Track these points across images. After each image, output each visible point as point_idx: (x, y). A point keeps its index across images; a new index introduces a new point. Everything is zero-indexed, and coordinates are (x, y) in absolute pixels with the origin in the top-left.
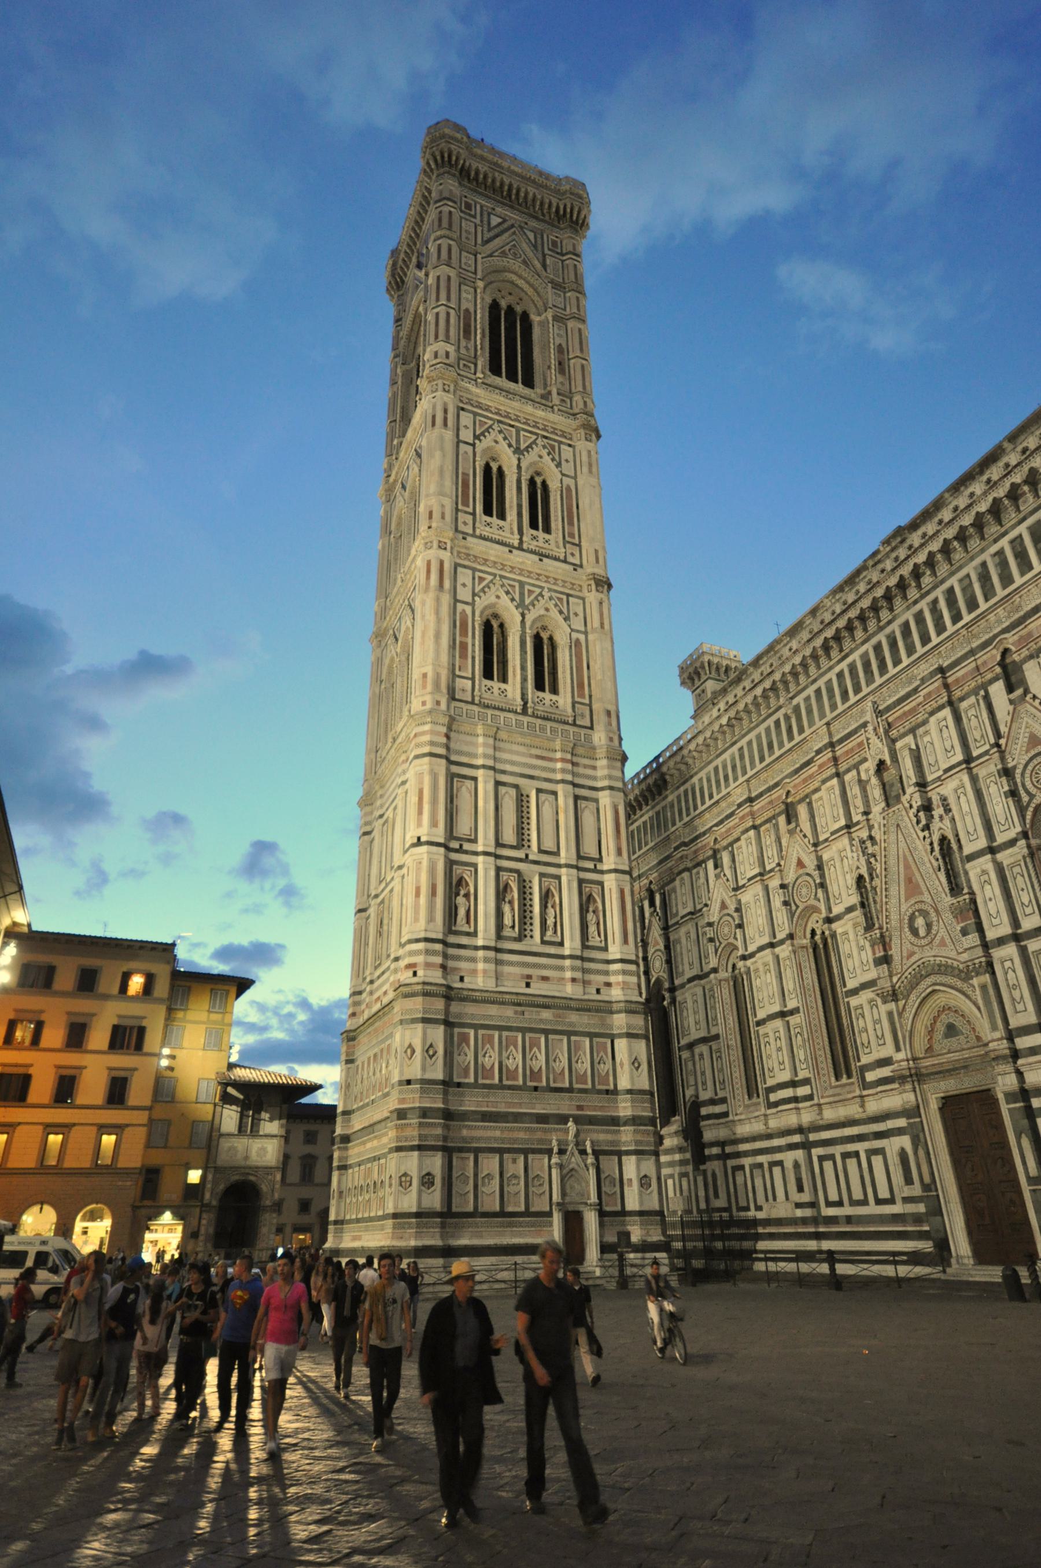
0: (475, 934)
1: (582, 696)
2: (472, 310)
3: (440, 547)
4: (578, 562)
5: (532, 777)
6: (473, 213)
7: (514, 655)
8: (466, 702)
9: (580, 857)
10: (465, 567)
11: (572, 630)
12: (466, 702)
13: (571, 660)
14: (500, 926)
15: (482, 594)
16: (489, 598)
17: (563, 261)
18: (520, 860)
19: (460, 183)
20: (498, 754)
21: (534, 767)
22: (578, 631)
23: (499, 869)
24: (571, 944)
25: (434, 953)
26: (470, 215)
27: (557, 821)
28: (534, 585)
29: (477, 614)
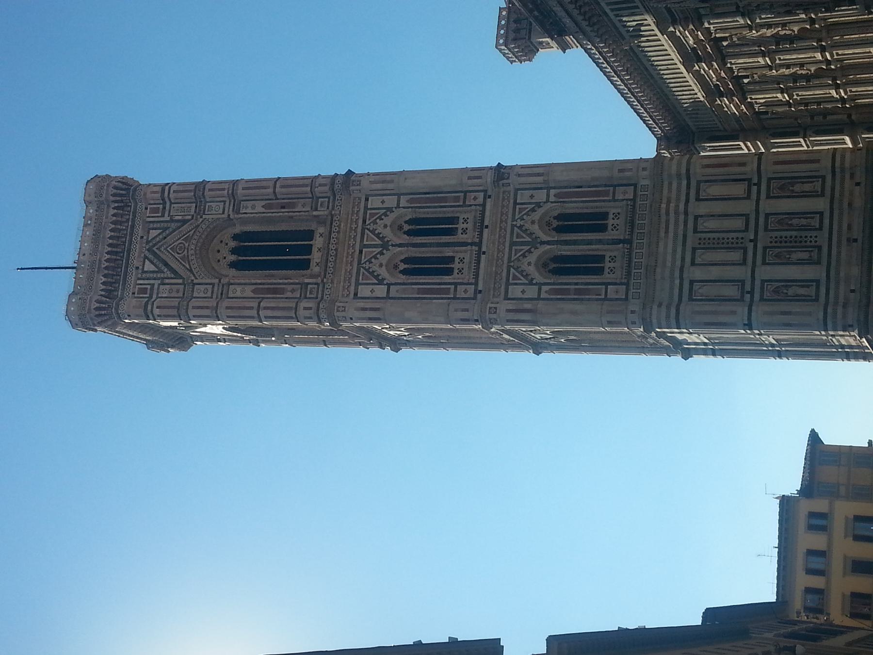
0: (818, 282)
3: (495, 313)
5: (685, 236)
7: (579, 250)
8: (627, 290)
9: (748, 197)
11: (547, 201)
12: (627, 290)
14: (810, 262)
15: (530, 278)
16: (531, 270)
17: (171, 203)
18: (755, 247)
19: (121, 299)
20: (669, 264)
22: (548, 195)
23: (764, 263)
24: (821, 204)
26: (152, 289)
27: (720, 216)
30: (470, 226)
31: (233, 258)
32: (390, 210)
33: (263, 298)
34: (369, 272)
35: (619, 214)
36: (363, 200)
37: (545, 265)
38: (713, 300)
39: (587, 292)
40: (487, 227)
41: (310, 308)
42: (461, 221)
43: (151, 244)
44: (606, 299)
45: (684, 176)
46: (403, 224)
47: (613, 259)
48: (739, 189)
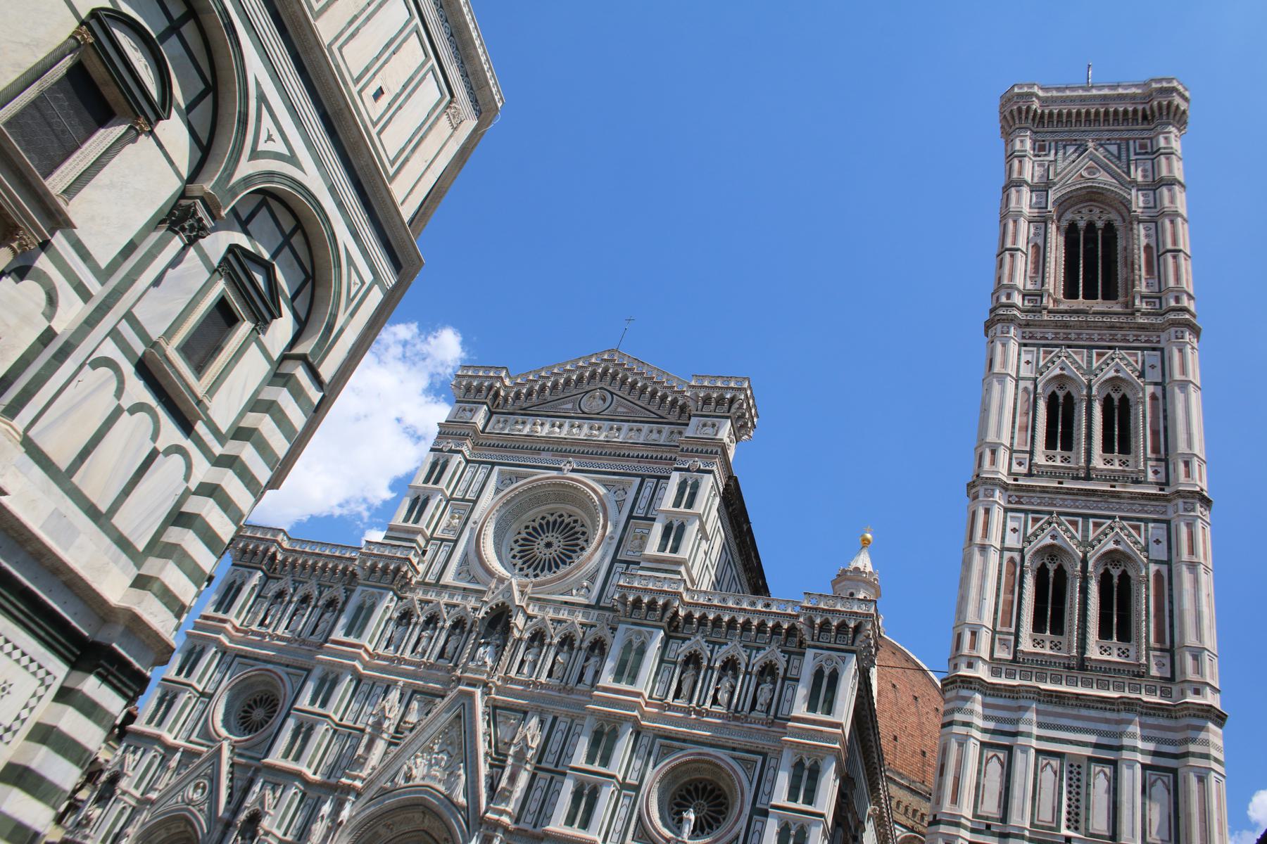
6: (1047, 152)
17: (1152, 159)
19: (1034, 132)
26: (1045, 155)
29: (1027, 558)
30: (1117, 466)
31: (1082, 224)
33: (1026, 255)
34: (1053, 357)
35: (1128, 656)
37: (1052, 559)
44: (994, 631)
45: (1181, 750)
46: (1121, 393)
47: (1055, 646)
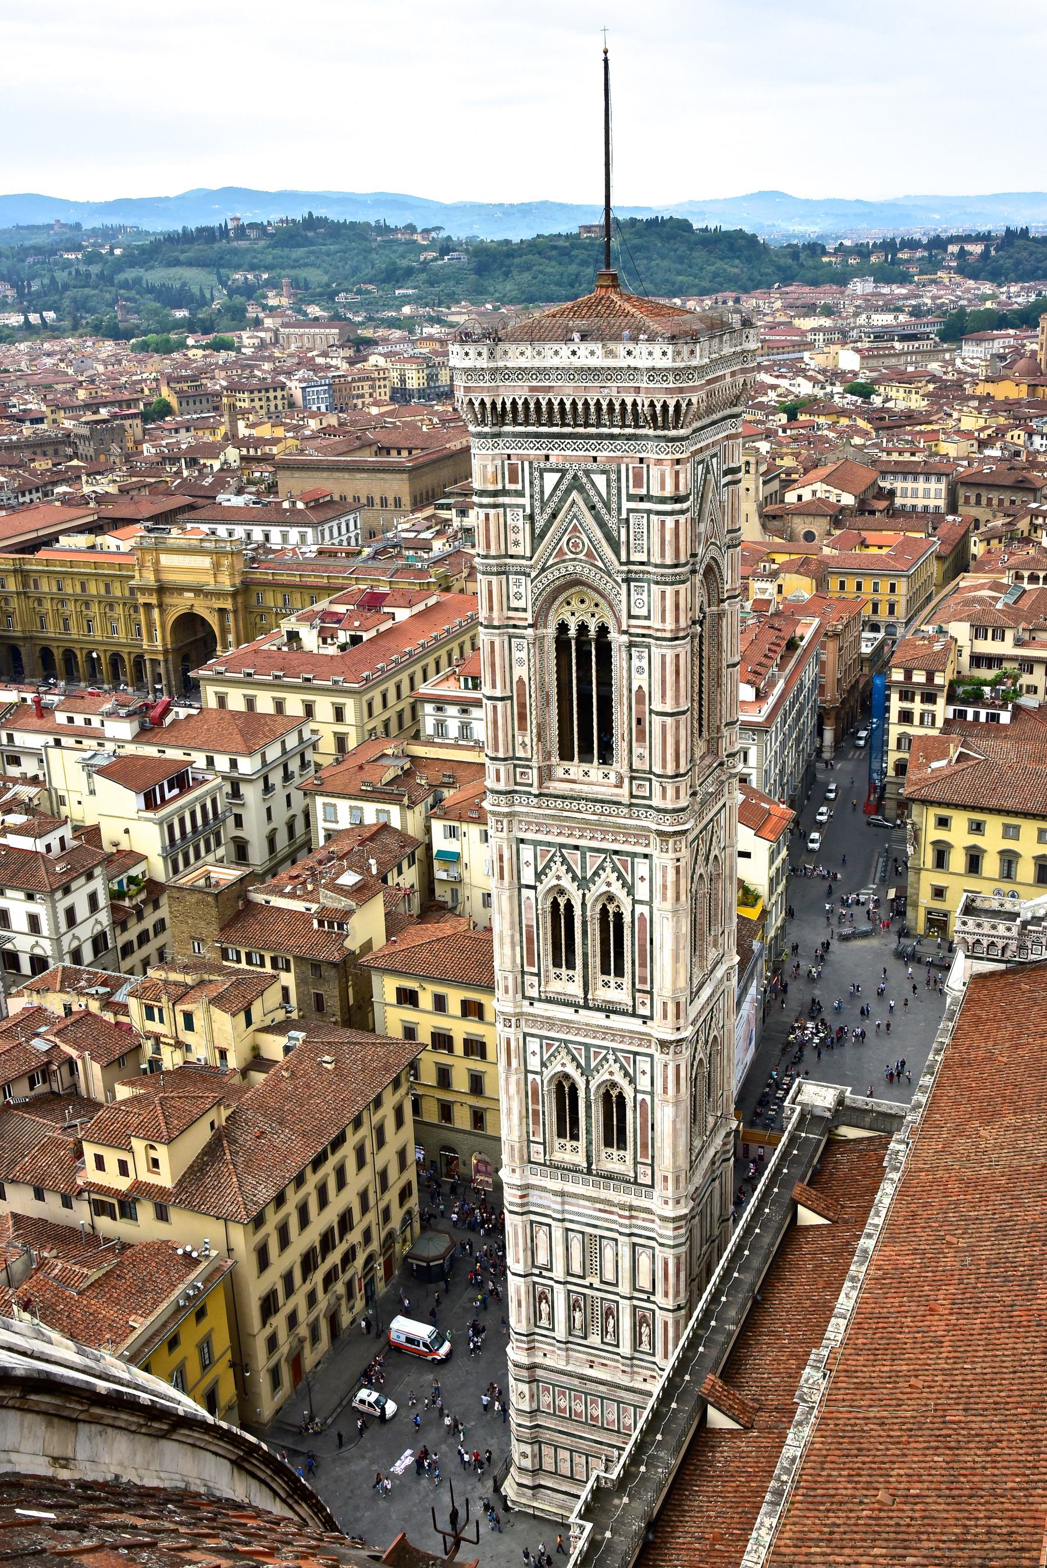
1: (644, 1155)
2: (526, 680)
4: (648, 1014)
6: (519, 487)
10: (532, 1035)
11: (636, 1091)
13: (635, 1123)
16: (556, 1068)
20: (567, 1207)
21: (598, 1218)
22: (644, 1092)
24: (626, 1349)
25: (522, 1341)
28: (600, 1047)
32: (630, 892)
36: (647, 851)
38: (532, 1241)
39: (536, 1122)
40: (608, 1017)
41: (498, 780)
42: (619, 980)
43: (584, 480)
44: (529, 1141)
48: (644, 1282)
